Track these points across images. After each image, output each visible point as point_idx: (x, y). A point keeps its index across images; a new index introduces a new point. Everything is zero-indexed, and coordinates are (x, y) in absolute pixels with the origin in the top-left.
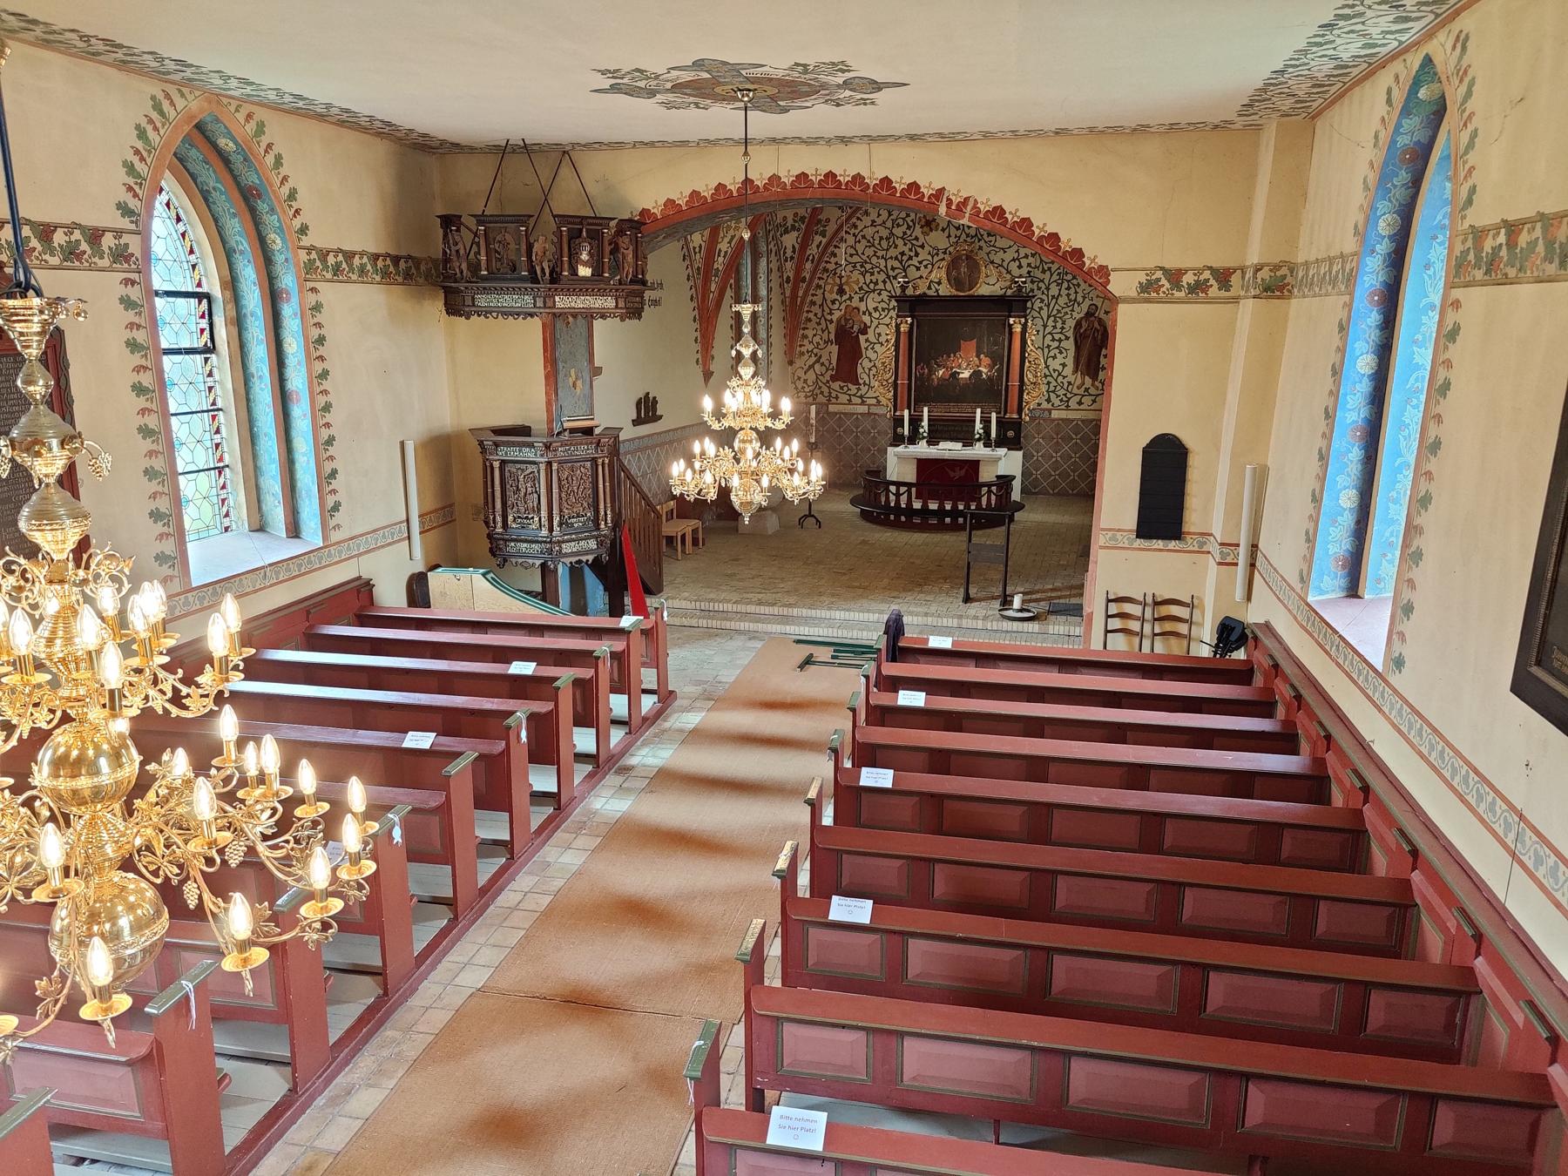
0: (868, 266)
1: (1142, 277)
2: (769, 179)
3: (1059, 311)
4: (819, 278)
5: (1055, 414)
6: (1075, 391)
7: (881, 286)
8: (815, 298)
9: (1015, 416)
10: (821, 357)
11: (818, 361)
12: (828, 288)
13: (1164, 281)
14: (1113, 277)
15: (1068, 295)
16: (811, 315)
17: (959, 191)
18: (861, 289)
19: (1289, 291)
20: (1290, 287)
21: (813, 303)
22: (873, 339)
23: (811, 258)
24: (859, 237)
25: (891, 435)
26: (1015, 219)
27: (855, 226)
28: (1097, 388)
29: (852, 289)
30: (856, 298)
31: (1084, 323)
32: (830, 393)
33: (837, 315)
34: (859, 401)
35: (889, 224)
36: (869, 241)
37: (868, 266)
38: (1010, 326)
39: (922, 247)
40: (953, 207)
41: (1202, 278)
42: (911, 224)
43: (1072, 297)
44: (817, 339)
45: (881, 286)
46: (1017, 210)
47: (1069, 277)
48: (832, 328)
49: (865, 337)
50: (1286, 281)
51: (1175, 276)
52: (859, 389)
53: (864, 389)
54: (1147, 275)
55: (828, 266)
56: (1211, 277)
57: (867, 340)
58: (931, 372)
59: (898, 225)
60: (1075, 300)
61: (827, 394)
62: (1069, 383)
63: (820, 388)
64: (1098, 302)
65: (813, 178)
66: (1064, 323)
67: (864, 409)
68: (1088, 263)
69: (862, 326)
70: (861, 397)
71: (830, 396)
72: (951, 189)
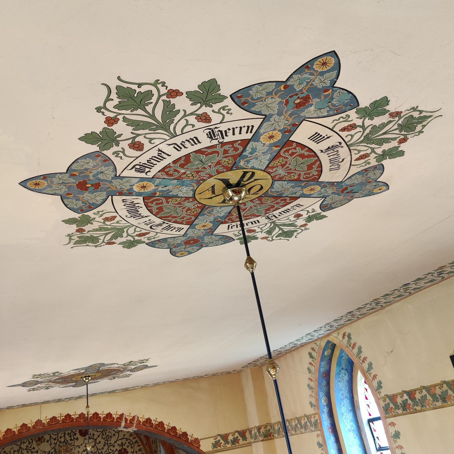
1: (212, 440)
2: (35, 423)
13: (221, 441)
14: (201, 443)
17: (130, 414)
19: (273, 436)
20: (272, 434)
26: (156, 423)
40: (128, 422)
41: (235, 436)
42: (31, 441)
46: (156, 419)
50: (270, 432)
51: (225, 437)
54: (214, 439)
56: (220, 439)
59: (24, 443)
65: (59, 419)
68: (190, 438)
72: (126, 413)
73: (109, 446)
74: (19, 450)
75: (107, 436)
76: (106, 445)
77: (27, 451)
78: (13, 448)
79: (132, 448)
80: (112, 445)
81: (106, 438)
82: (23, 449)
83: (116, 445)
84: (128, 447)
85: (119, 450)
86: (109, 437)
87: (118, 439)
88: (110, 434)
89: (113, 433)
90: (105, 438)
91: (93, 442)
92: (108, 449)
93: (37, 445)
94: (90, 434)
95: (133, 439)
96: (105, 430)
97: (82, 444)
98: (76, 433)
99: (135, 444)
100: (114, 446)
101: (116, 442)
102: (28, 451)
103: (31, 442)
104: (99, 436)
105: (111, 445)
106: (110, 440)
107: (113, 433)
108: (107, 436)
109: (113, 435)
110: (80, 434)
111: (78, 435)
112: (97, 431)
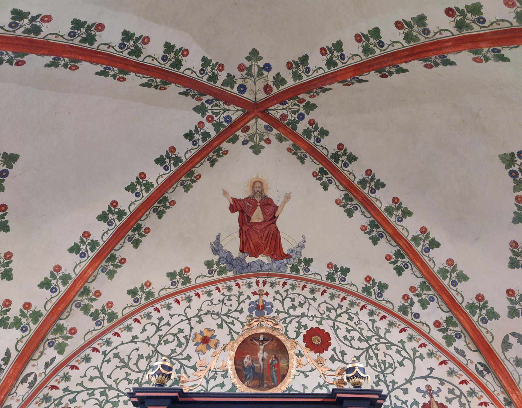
24: (111, 355)
35: (155, 340)
42: (183, 341)
59: (167, 342)
74: (152, 357)
75: (380, 361)
78: (137, 350)
80: (399, 388)
83: (412, 388)
86: (387, 365)
93: (197, 351)
94: (334, 350)
96: (374, 347)
97: (312, 370)
100: (406, 391)
101: (409, 381)
102: (174, 361)
103: (184, 343)
104: (358, 358)
105: (396, 386)
106: (392, 373)
108: (380, 361)
112: (352, 347)
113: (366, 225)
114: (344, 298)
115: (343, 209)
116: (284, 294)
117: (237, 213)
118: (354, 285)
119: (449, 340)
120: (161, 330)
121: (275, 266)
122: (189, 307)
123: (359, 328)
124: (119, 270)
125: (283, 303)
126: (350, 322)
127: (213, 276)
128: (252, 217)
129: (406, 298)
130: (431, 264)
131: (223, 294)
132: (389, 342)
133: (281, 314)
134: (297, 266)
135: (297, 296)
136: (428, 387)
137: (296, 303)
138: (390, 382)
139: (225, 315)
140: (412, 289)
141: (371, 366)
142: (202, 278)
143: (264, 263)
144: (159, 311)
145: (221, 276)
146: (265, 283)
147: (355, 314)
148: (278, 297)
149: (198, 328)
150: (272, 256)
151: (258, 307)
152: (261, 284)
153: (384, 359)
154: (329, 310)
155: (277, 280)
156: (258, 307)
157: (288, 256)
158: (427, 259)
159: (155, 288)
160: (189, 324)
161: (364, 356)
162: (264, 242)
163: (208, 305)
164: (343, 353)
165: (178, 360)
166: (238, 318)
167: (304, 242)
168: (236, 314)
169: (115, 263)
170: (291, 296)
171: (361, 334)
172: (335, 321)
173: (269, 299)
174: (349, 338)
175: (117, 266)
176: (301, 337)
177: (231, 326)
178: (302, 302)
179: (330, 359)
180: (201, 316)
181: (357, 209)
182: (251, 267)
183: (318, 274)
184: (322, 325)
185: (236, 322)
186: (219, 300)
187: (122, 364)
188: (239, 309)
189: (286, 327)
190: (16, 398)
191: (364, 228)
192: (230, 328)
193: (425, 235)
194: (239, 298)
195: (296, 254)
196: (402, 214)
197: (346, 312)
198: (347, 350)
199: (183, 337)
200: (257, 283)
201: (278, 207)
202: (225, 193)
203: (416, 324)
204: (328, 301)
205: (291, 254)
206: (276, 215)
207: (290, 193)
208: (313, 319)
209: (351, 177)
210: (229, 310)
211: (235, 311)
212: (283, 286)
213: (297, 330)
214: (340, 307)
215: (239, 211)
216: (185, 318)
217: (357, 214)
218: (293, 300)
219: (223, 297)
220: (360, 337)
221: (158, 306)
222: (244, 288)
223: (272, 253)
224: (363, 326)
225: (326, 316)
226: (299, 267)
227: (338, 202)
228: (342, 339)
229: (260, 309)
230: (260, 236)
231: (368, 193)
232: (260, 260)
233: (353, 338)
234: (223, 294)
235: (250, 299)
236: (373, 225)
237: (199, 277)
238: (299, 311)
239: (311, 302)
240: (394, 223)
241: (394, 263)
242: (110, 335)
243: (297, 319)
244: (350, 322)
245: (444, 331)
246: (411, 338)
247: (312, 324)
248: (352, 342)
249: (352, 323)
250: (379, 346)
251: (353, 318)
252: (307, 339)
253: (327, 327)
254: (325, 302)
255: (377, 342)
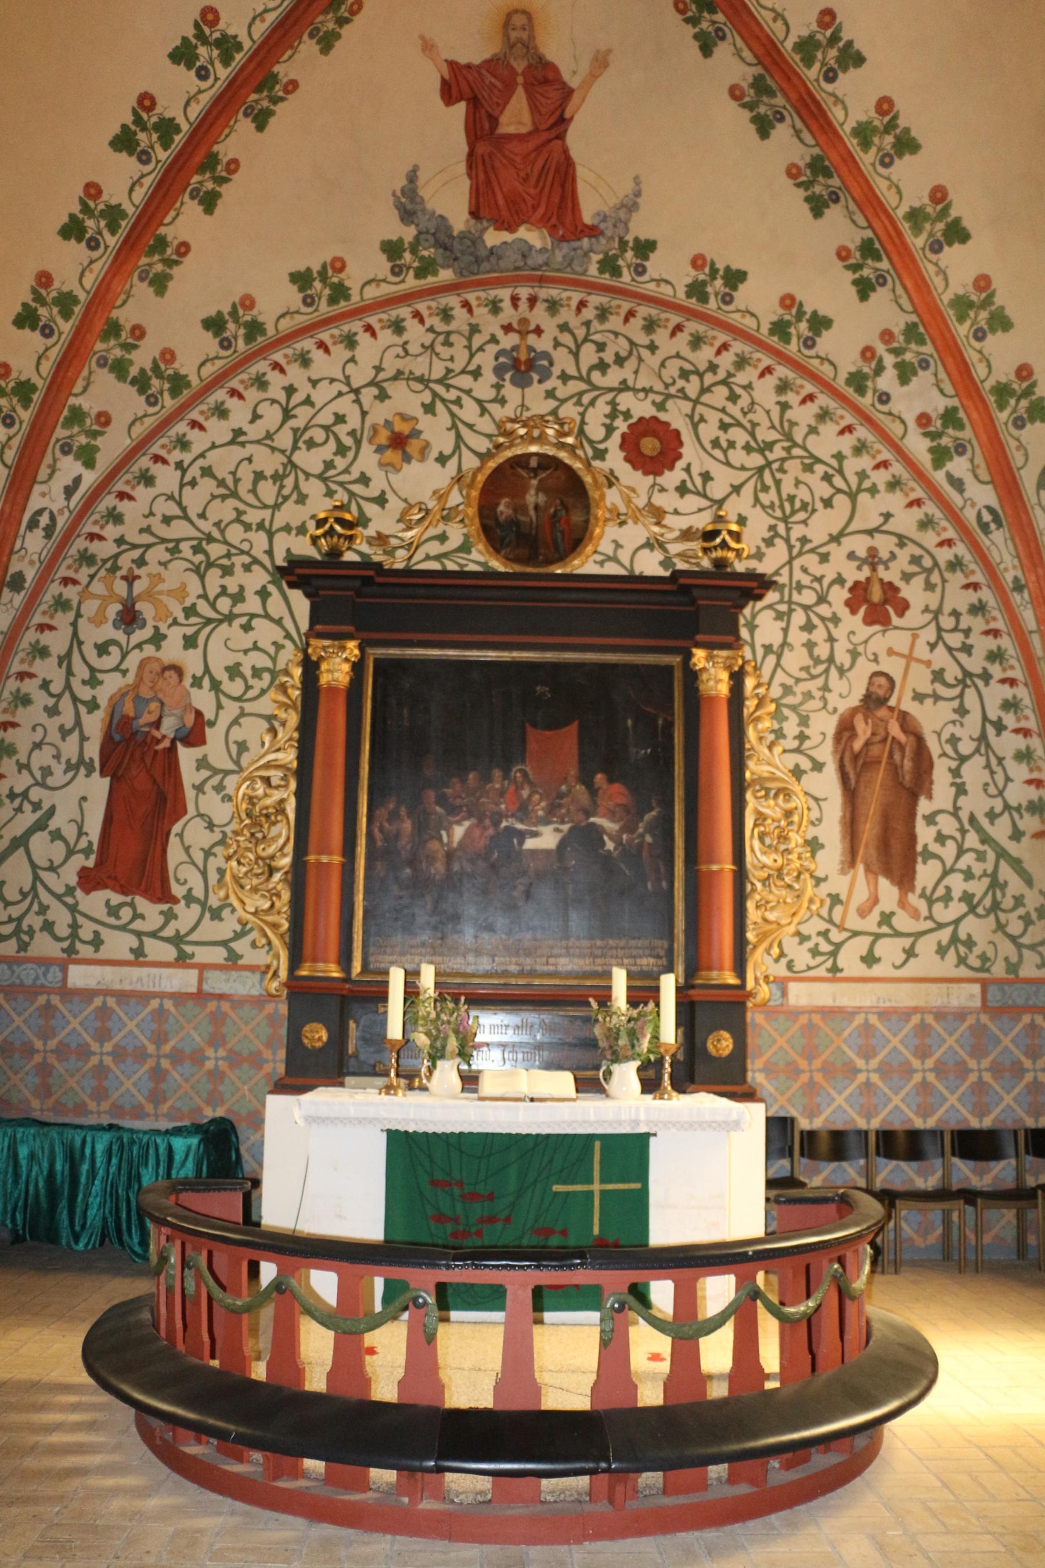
0: (215, 550)
3: (787, 690)
4: (66, 581)
5: (800, 995)
6: (854, 922)
7: (252, 604)
8: (46, 638)
9: (732, 980)
10: (51, 812)
11: (40, 826)
12: (90, 608)
15: (810, 645)
16: (30, 687)
18: (190, 611)
21: (42, 652)
22: (220, 759)
23: (44, 520)
24: (194, 472)
25: (277, 1063)
27: (183, 444)
28: (915, 915)
29: (163, 612)
30: (175, 637)
31: (863, 730)
32: (75, 926)
33: (112, 685)
34: (169, 953)
35: (285, 439)
36: (221, 483)
37: (215, 550)
38: (692, 677)
39: (381, 500)
42: (348, 441)
43: (822, 650)
44: (42, 758)
45: (252, 604)
47: (808, 597)
48: (94, 724)
49: (197, 752)
52: (170, 916)
53: (186, 916)
55: (95, 547)
57: (202, 763)
58: (426, 828)
59: (311, 444)
60: (831, 660)
61: (62, 930)
62: (835, 899)
63: (43, 909)
64: (893, 667)
66: (804, 721)
67: (184, 980)
69: (190, 720)
70: (177, 940)
71: (74, 935)
73: (795, 551)
74: (285, 476)
75: (784, 497)
76: (778, 542)
77: (327, 486)
79: (929, 586)
80: (812, 551)
81: (782, 507)
82: (308, 475)
83: (838, 553)
84: (907, 577)
85: (857, 584)
86: (798, 504)
87: (850, 529)
88: (803, 494)
89: (826, 491)
90: (772, 506)
91: (700, 510)
92: (790, 562)
93: (381, 465)
94: (688, 469)
95: (941, 544)
96: (775, 466)
98: (606, 450)
99: (947, 575)
100: (824, 558)
101: (836, 539)
103: (350, 448)
104: (737, 489)
105: (808, 547)
107: (826, 491)
108: (784, 497)
109: (822, 499)
110: (627, 459)
111: (615, 460)
112: (728, 464)
113: (802, 164)
114: (725, 347)
115: (747, 114)
116: (581, 333)
117: (461, 108)
118: (753, 315)
119: (940, 456)
120: (295, 416)
121: (559, 256)
122: (352, 360)
123: (750, 421)
124: (176, 271)
125: (576, 355)
126: (731, 408)
127: (403, 281)
128: (503, 119)
129: (868, 354)
130: (938, 282)
131: (431, 330)
132: (812, 456)
133: (571, 383)
134: (616, 257)
135: (612, 336)
136: (873, 552)
137: (608, 357)
138: (798, 539)
139: (439, 381)
140: (887, 336)
141: (763, 507)
142: (378, 286)
143: (531, 247)
144: (282, 371)
145: (422, 282)
146: (533, 301)
147: (744, 387)
148: (566, 339)
149: (380, 413)
150: (552, 230)
151: (516, 363)
152: (523, 305)
153: (793, 491)
154: (684, 374)
155: (565, 295)
156: (516, 363)
157: (593, 231)
158: (932, 269)
159: (267, 311)
160: (358, 401)
161: (751, 484)
162: (532, 191)
163: (398, 356)
164: (706, 477)
165: (341, 484)
166: (471, 390)
167: (638, 194)
168: (465, 381)
169: (166, 256)
170: (597, 337)
171: (753, 435)
172: (696, 402)
173: (543, 344)
174: (724, 444)
175: (170, 263)
176: (616, 438)
177: (455, 408)
178: (623, 354)
179: (677, 489)
180: (385, 385)
181: (782, 119)
182: (500, 258)
183: (667, 282)
184: (666, 410)
185: (466, 400)
186: (423, 346)
187: (222, 491)
188: (471, 368)
189: (583, 415)
190: (27, 560)
191: (794, 171)
192: (453, 415)
193: (939, 207)
194: (469, 339)
195: (615, 226)
196: (894, 146)
197: (724, 382)
198: (717, 470)
199: (348, 434)
200: (515, 300)
201: (571, 91)
202: (428, 47)
203: (881, 416)
204: (686, 352)
205: (602, 226)
206: (567, 115)
207: (609, 51)
208: (646, 396)
209: (778, 28)
210: (449, 371)
211: (463, 372)
212: (579, 310)
213: (608, 421)
214: (713, 368)
215: (468, 100)
216: (345, 389)
217: (782, 132)
218: (601, 347)
219: (431, 336)
220: (748, 443)
221: (278, 357)
222: (481, 313)
223: (554, 221)
224: (759, 416)
225: (679, 391)
226: (621, 262)
227: (737, 93)
228: (708, 446)
229: (523, 368)
230: (522, 174)
231: (817, 80)
232: (521, 240)
233: (732, 444)
234: (431, 330)
235: (497, 342)
236: (818, 167)
237: (369, 282)
238: (614, 377)
239: (645, 353)
240: (871, 168)
241: (855, 268)
242: (181, 427)
243: (609, 396)
244: (731, 408)
245: (933, 436)
246: (860, 449)
247: (642, 408)
248: (731, 452)
249: (735, 410)
250: (787, 465)
251: (739, 396)
252: (631, 446)
253: (675, 416)
254: (678, 356)
255: (784, 454)
